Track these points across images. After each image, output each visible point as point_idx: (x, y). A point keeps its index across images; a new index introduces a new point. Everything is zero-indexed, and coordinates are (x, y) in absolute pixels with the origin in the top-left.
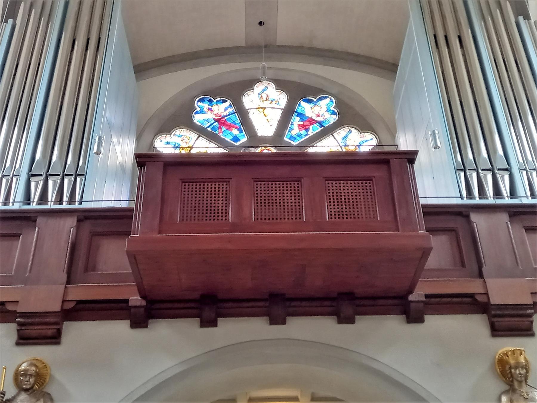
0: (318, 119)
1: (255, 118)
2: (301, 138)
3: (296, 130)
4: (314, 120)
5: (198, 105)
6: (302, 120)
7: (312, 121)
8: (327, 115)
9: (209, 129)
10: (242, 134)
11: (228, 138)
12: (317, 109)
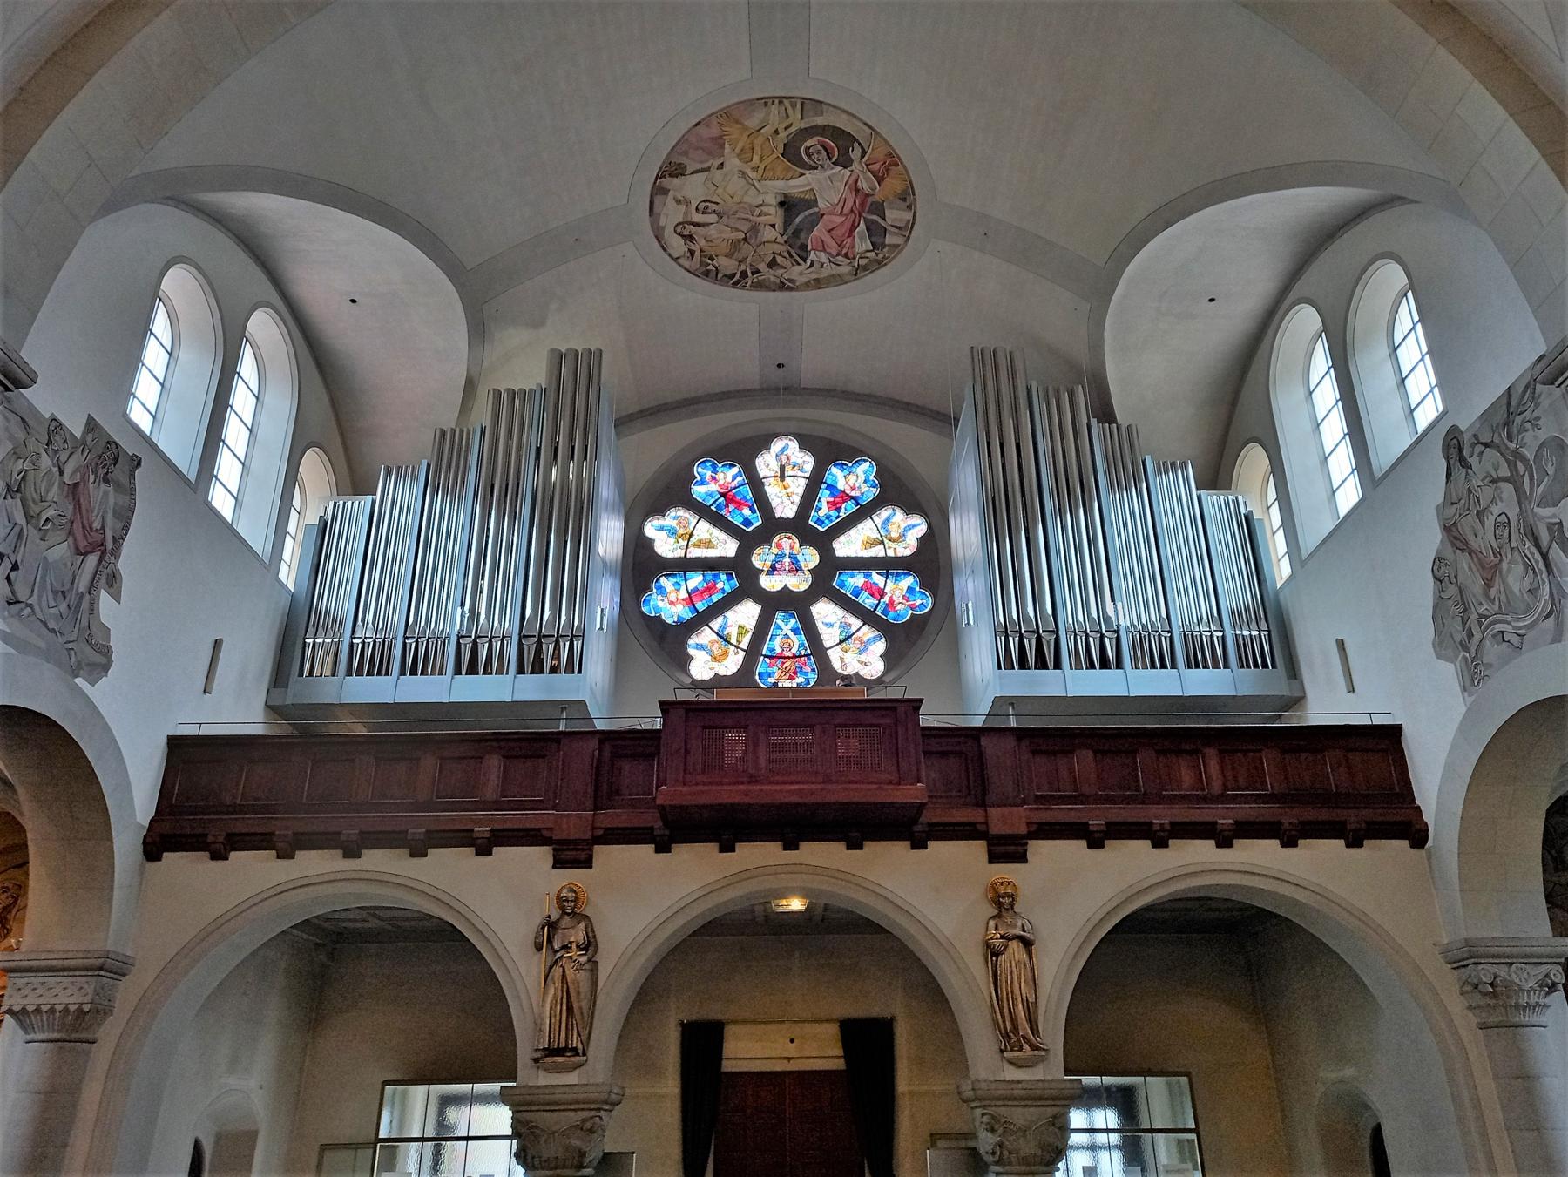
0: (853, 494)
1: (772, 490)
3: (824, 511)
5: (698, 470)
6: (832, 495)
7: (845, 497)
8: (865, 488)
11: (738, 521)
12: (852, 479)
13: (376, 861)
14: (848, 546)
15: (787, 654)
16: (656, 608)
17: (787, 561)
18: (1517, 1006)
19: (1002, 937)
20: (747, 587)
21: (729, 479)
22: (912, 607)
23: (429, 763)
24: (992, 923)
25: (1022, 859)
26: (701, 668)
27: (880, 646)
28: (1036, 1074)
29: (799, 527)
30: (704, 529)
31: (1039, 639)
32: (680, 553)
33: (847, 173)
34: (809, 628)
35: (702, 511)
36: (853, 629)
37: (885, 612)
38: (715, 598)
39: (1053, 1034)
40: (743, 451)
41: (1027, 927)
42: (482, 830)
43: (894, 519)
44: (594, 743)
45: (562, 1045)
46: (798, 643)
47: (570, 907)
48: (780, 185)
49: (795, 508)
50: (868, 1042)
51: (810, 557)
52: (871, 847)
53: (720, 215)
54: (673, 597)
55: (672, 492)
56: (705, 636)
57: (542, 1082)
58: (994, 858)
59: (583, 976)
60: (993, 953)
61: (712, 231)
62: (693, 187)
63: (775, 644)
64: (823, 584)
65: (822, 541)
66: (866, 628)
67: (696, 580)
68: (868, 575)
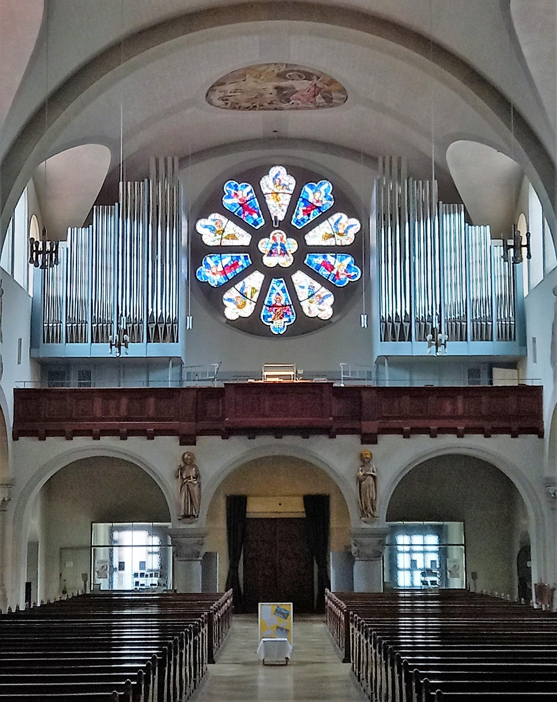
0: (318, 205)
1: (270, 202)
2: (304, 222)
4: (314, 205)
5: (226, 188)
6: (305, 206)
9: (236, 214)
10: (260, 219)
11: (250, 222)
12: (317, 194)
13: (106, 441)
14: (314, 238)
15: (278, 304)
16: (206, 277)
17: (279, 248)
19: (364, 475)
20: (256, 264)
21: (245, 195)
22: (349, 276)
23: (124, 401)
24: (360, 468)
25: (376, 442)
26: (232, 312)
27: (331, 300)
29: (286, 226)
30: (231, 227)
31: (402, 325)
32: (217, 243)
33: (311, 82)
34: (291, 289)
36: (316, 290)
37: (334, 280)
38: (238, 270)
39: (382, 510)
40: (253, 176)
41: (375, 470)
43: (341, 222)
44: (194, 393)
46: (284, 298)
47: (188, 462)
48: (276, 84)
49: (284, 214)
50: (318, 507)
51: (292, 245)
52: (313, 439)
54: (214, 270)
55: (212, 203)
56: (232, 294)
57: (181, 527)
58: (363, 442)
59: (196, 489)
60: (360, 481)
61: (239, 97)
62: (229, 88)
63: (271, 298)
64: (299, 262)
65: (299, 235)
66: (323, 288)
67: (227, 259)
68: (325, 257)
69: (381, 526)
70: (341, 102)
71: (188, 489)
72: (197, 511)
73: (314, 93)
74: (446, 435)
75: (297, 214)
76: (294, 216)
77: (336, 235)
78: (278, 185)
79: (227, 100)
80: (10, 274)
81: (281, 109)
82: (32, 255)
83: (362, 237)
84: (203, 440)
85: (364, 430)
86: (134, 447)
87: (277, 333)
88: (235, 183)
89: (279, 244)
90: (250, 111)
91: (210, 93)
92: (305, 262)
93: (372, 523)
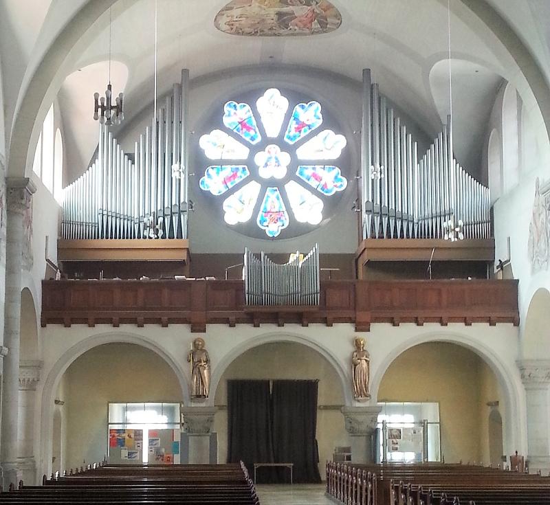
0: (307, 123)
3: (293, 132)
5: (226, 108)
11: (248, 139)
14: (303, 153)
17: (273, 161)
18: (536, 382)
22: (335, 186)
24: (355, 354)
28: (367, 404)
33: (309, 8)
35: (229, 132)
37: (323, 189)
38: (237, 181)
42: (165, 319)
45: (201, 394)
48: (278, 9)
51: (285, 158)
53: (247, 18)
55: (214, 121)
58: (357, 330)
61: (243, 22)
64: (291, 175)
67: (227, 171)
69: (372, 405)
70: (335, 27)
71: (199, 371)
72: (207, 392)
73: (310, 20)
74: (430, 324)
75: (289, 132)
76: (287, 133)
77: (324, 150)
78: (273, 104)
79: (232, 25)
80: (39, 176)
81: (279, 35)
82: (96, 111)
83: (347, 153)
84: (211, 328)
85: (358, 320)
86: (151, 334)
87: (271, 236)
88: (235, 103)
89: (273, 157)
90: (253, 37)
91: (219, 17)
92: (297, 174)
93: (365, 401)
